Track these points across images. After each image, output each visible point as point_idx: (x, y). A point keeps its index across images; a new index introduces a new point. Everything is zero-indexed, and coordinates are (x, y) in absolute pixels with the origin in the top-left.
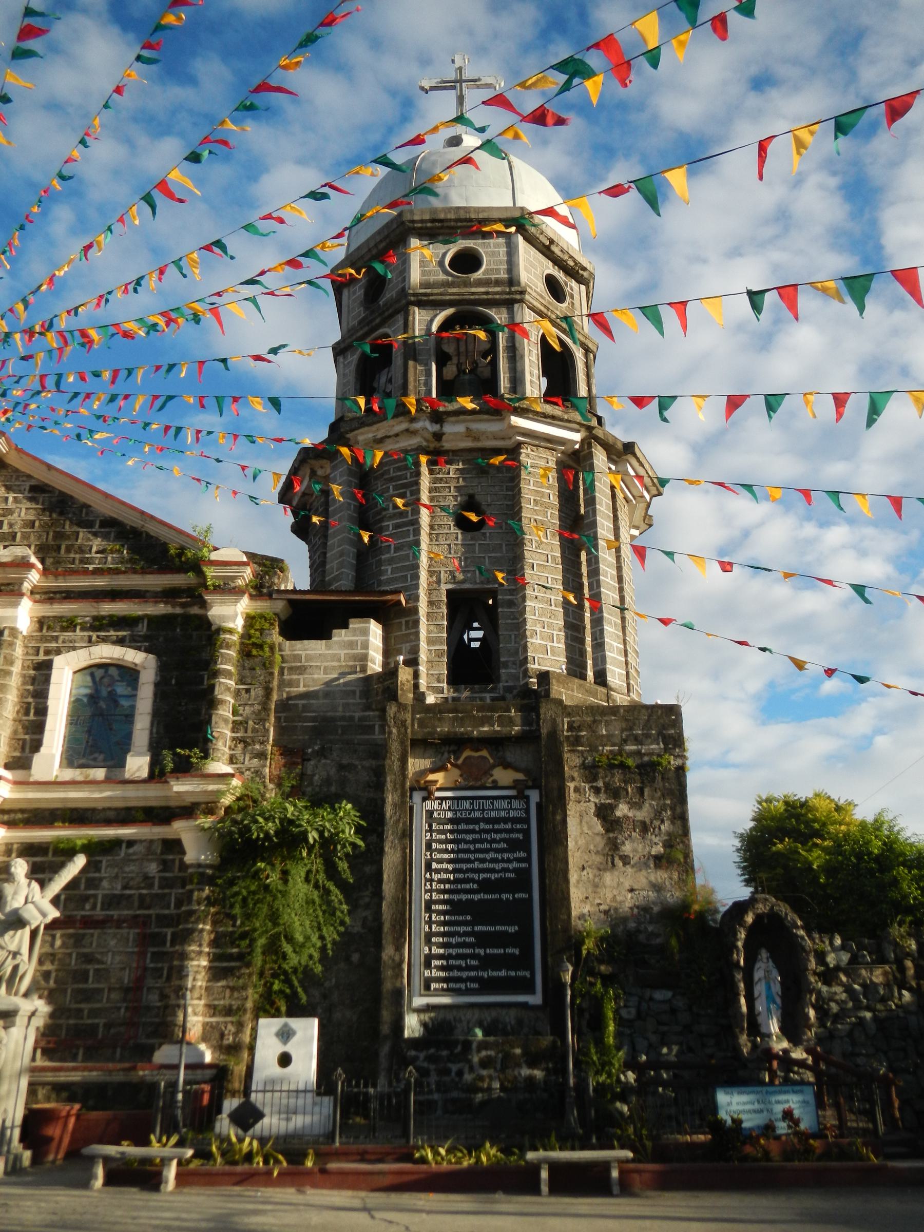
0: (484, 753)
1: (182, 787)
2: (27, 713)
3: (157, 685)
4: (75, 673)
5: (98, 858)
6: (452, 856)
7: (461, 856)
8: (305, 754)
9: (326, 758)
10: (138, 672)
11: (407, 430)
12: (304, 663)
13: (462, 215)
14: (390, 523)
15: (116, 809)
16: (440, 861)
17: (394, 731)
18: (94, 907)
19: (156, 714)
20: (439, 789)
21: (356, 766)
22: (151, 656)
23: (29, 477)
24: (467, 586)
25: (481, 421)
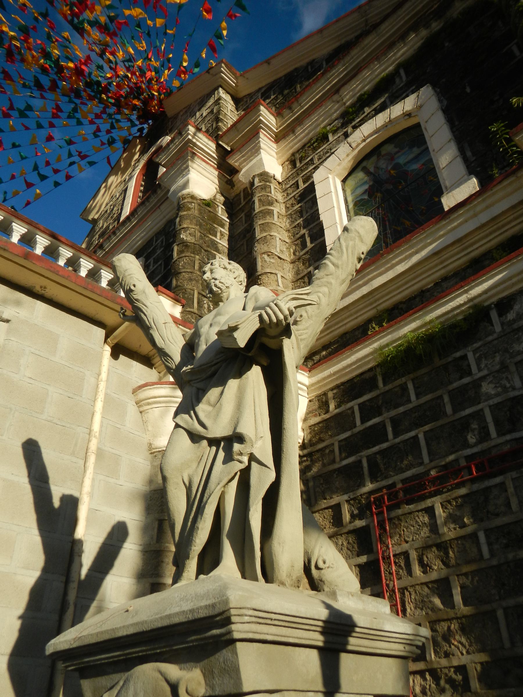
2: (304, 245)
4: (344, 181)
5: (458, 354)
18: (484, 435)
23: (260, 89)
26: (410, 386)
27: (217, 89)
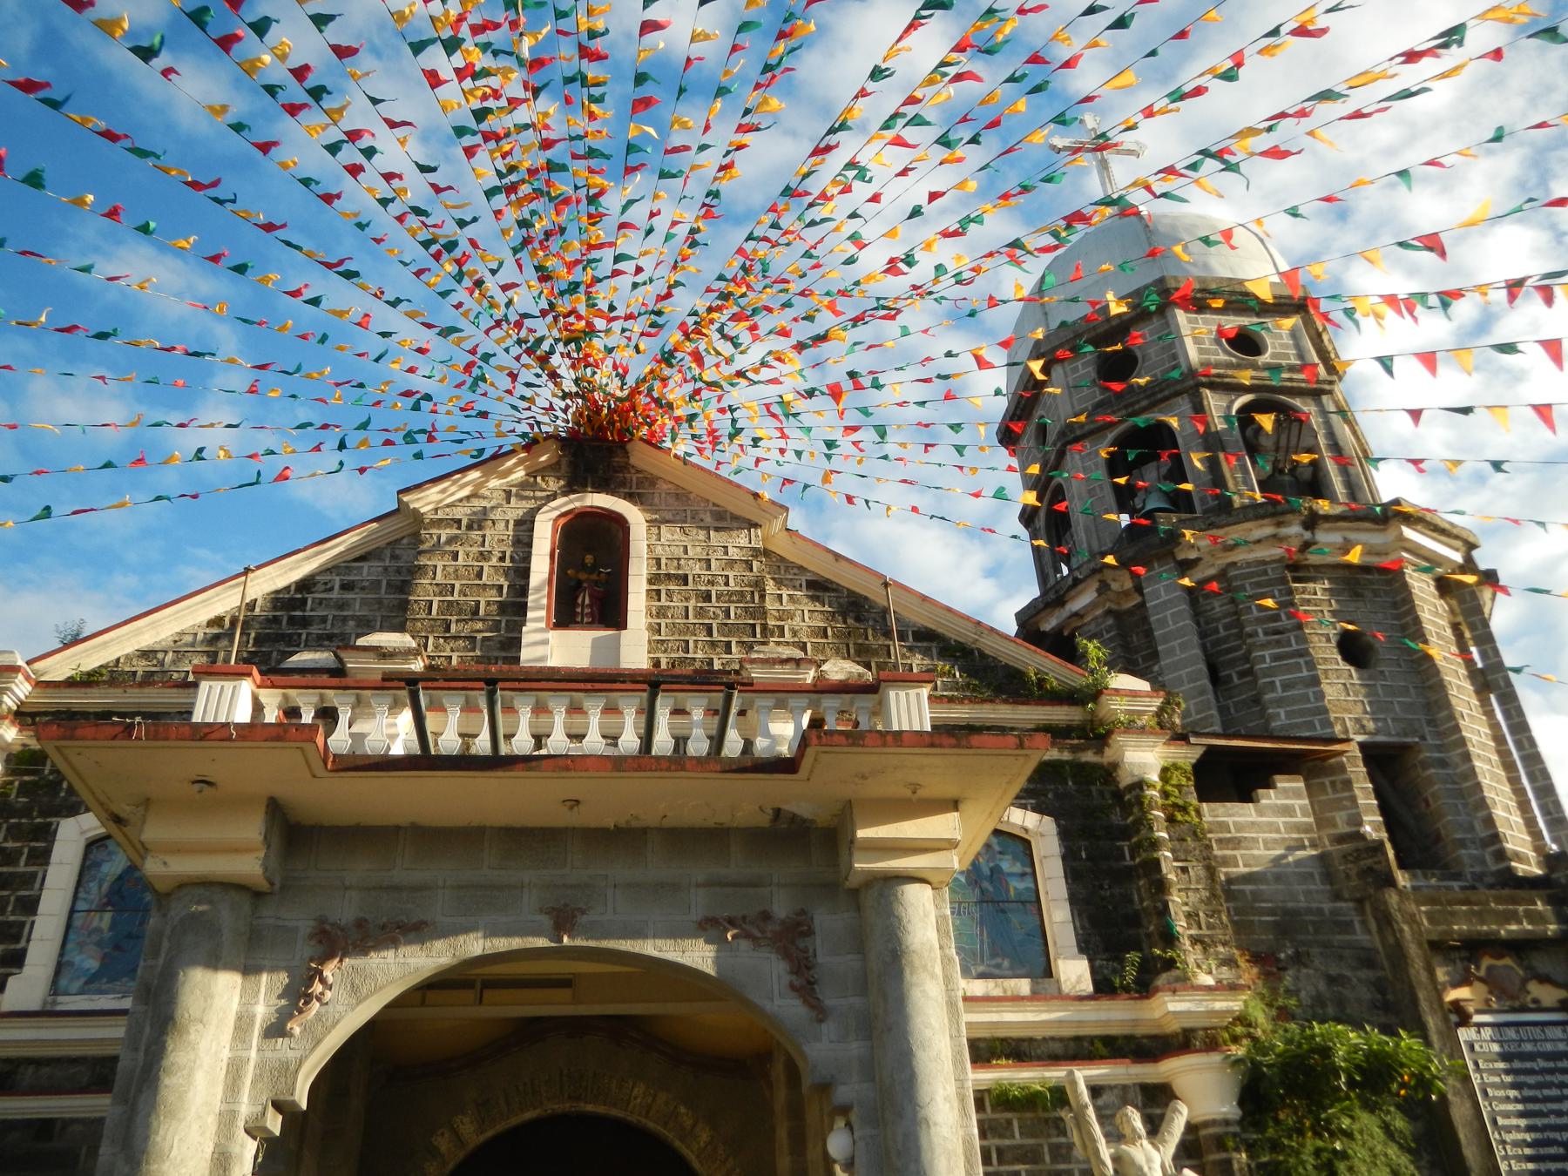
0: (1507, 961)
1: (1172, 1008)
3: (1064, 858)
6: (1520, 1107)
7: (1531, 1106)
8: (1278, 960)
9: (1306, 966)
10: (1027, 844)
11: (1274, 536)
12: (1234, 834)
13: (1238, 288)
14: (1267, 653)
15: (1061, 1040)
16: (1506, 1115)
17: (1406, 928)
19: (1073, 900)
20: (1479, 1012)
21: (1349, 980)
22: (1047, 819)
23: (801, 568)
24: (1381, 738)
25: (1358, 530)
26: (1015, 1124)
27: (756, 526)
